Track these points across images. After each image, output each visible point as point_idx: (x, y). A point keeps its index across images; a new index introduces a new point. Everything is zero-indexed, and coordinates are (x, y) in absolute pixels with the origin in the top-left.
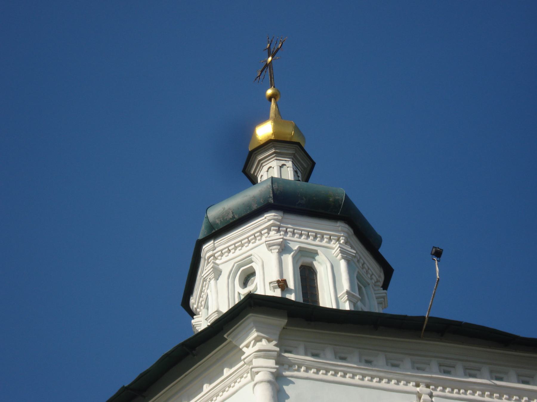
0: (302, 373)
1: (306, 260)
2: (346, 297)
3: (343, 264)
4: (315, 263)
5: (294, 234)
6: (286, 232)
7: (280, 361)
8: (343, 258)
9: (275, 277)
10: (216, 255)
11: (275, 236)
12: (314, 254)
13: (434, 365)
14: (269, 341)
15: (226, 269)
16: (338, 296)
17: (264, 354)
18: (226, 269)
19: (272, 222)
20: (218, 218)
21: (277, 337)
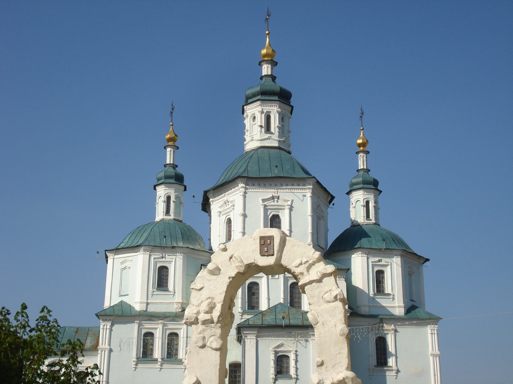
0: (250, 190)
1: (268, 114)
2: (277, 127)
3: (277, 115)
4: (270, 114)
5: (265, 106)
6: (263, 106)
7: (246, 189)
8: (277, 113)
9: (259, 124)
10: (247, 110)
11: (260, 109)
12: (271, 112)
13: (279, 185)
14: (243, 183)
15: (250, 115)
16: (275, 126)
17: (242, 187)
18: (250, 115)
19: (259, 104)
20: (248, 96)
21: (245, 182)
